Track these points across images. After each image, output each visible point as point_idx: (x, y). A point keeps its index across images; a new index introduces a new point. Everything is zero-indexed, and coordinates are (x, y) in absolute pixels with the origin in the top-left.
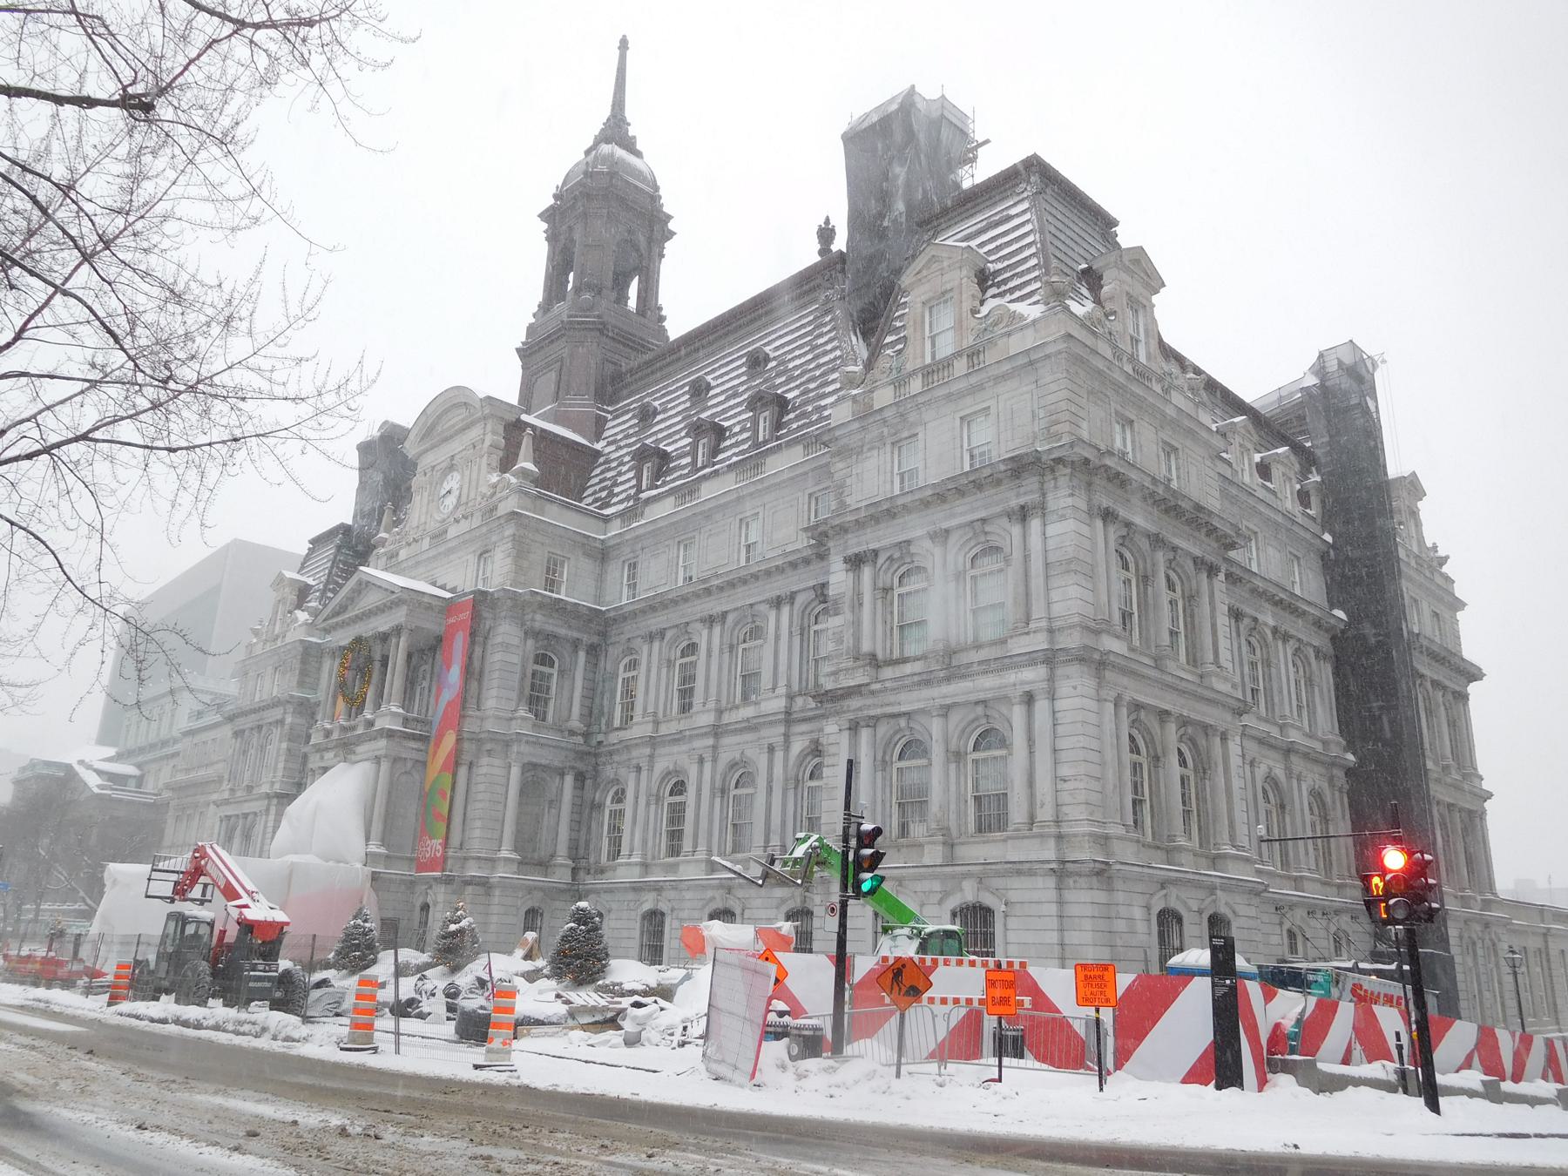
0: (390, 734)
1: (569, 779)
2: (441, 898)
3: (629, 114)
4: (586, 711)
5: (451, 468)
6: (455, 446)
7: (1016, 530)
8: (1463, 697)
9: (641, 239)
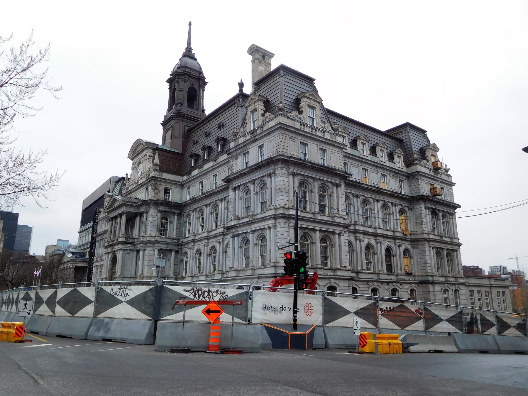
0: (122, 243)
1: (173, 253)
3: (193, 46)
4: (178, 233)
5: (140, 163)
6: (140, 156)
7: (269, 179)
8: (453, 214)
9: (196, 86)
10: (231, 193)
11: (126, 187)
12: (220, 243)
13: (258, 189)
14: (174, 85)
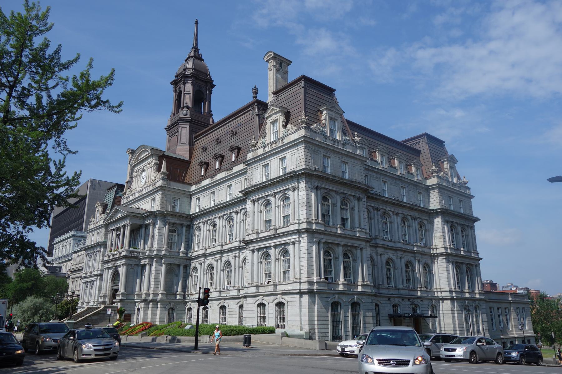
0: (125, 257)
2: (143, 306)
3: (199, 47)
4: (186, 246)
5: (144, 170)
9: (203, 89)
10: (249, 205)
11: (127, 196)
12: (235, 257)
13: (280, 203)
14: (180, 87)
